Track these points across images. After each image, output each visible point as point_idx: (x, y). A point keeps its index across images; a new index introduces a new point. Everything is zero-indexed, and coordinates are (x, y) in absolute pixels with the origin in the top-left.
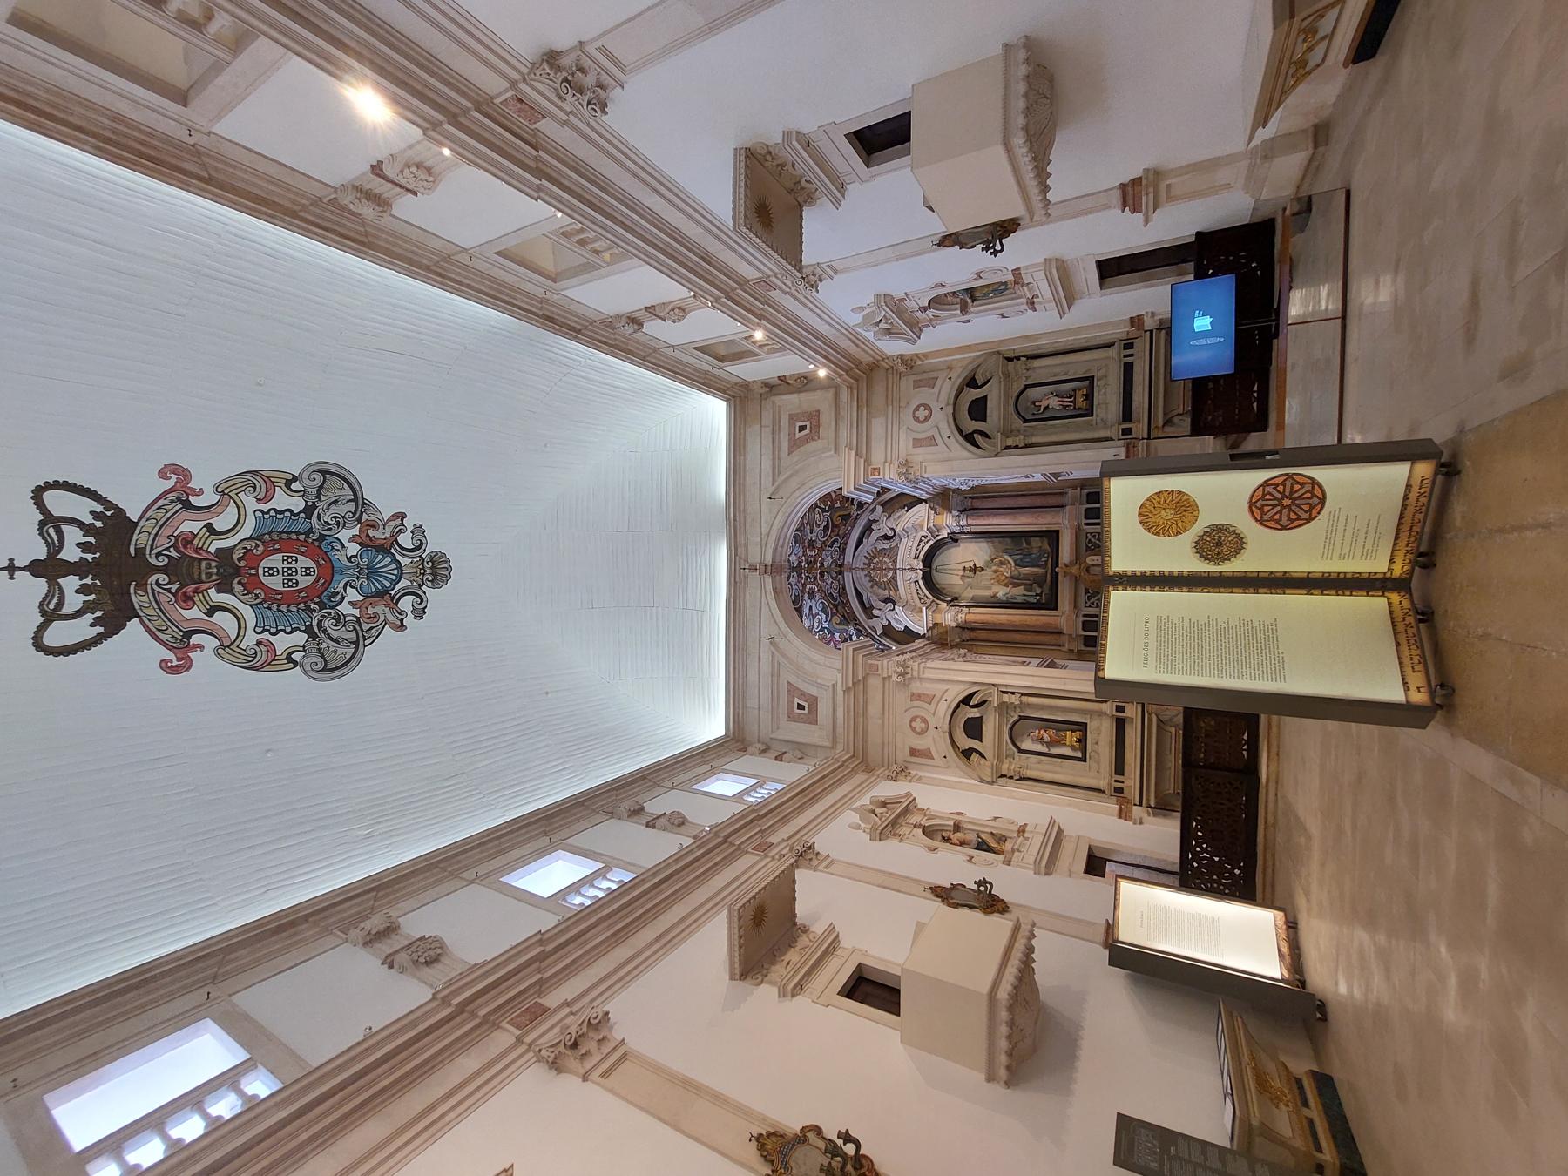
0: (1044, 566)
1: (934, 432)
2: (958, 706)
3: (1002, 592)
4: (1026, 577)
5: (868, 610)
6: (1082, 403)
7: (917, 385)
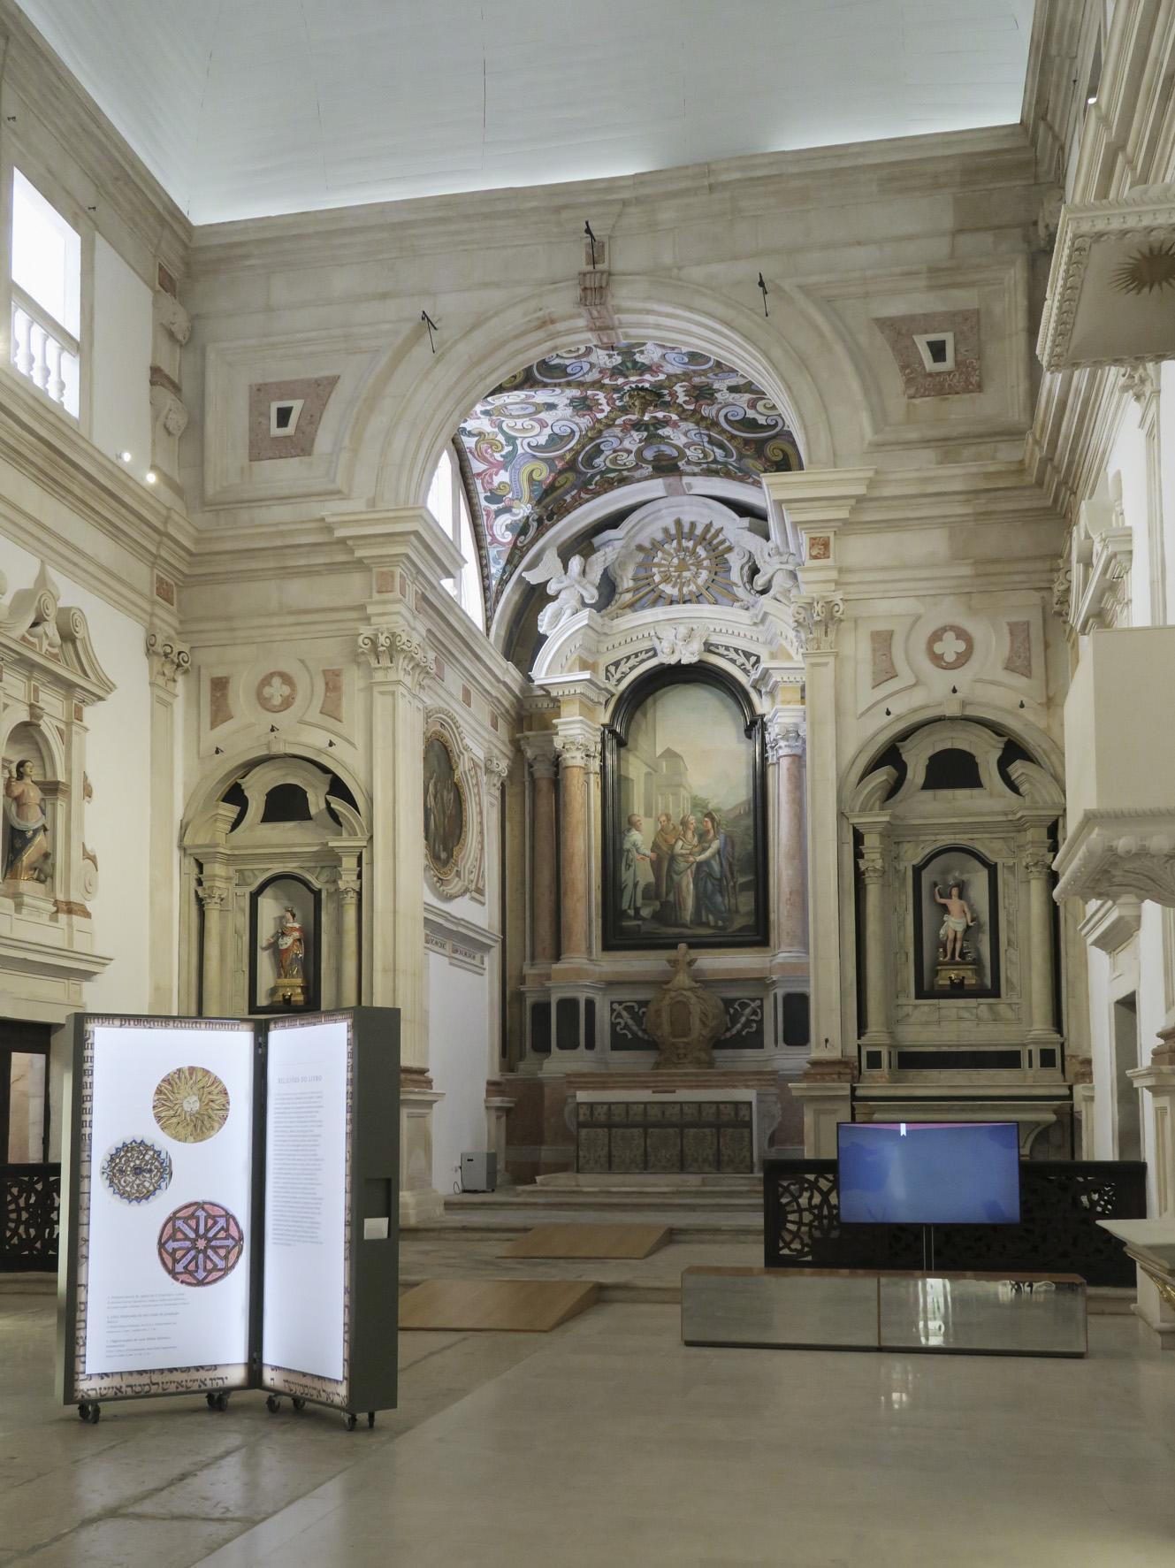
0: (698, 921)
1: (906, 677)
2: (325, 770)
3: (640, 839)
4: (674, 887)
5: (583, 544)
6: (949, 975)
7: (1018, 631)
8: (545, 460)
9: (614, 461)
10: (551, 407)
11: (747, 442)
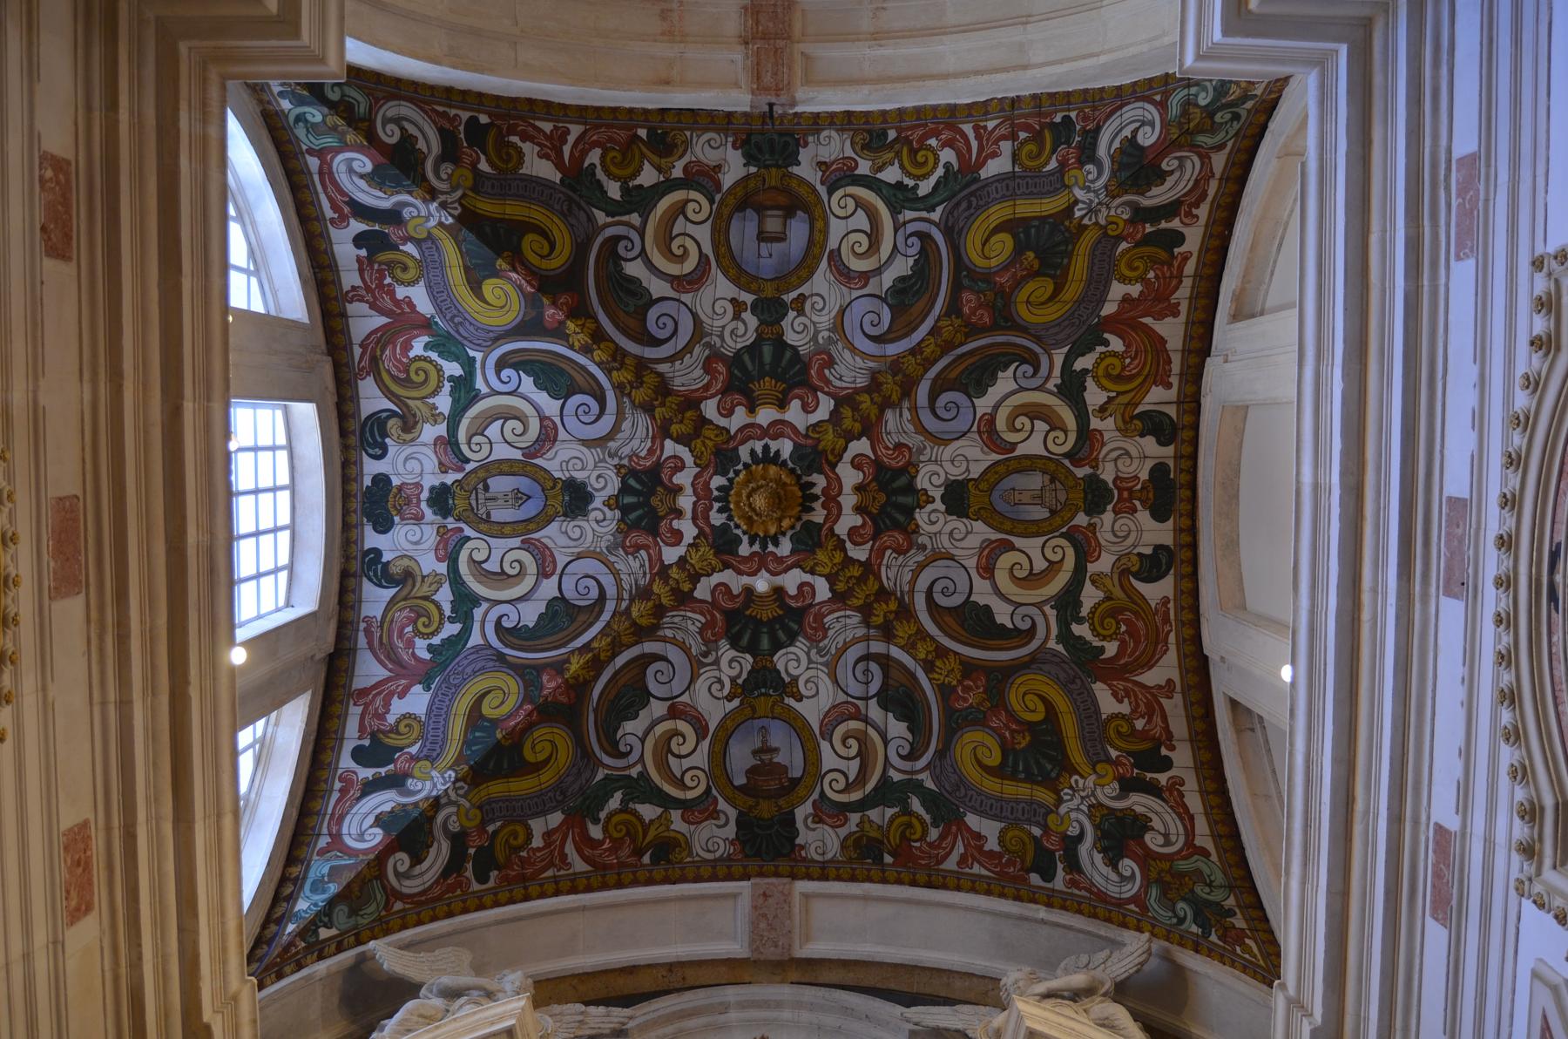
8: (519, 669)
9: (664, 750)
10: (575, 498)
11: (969, 668)
